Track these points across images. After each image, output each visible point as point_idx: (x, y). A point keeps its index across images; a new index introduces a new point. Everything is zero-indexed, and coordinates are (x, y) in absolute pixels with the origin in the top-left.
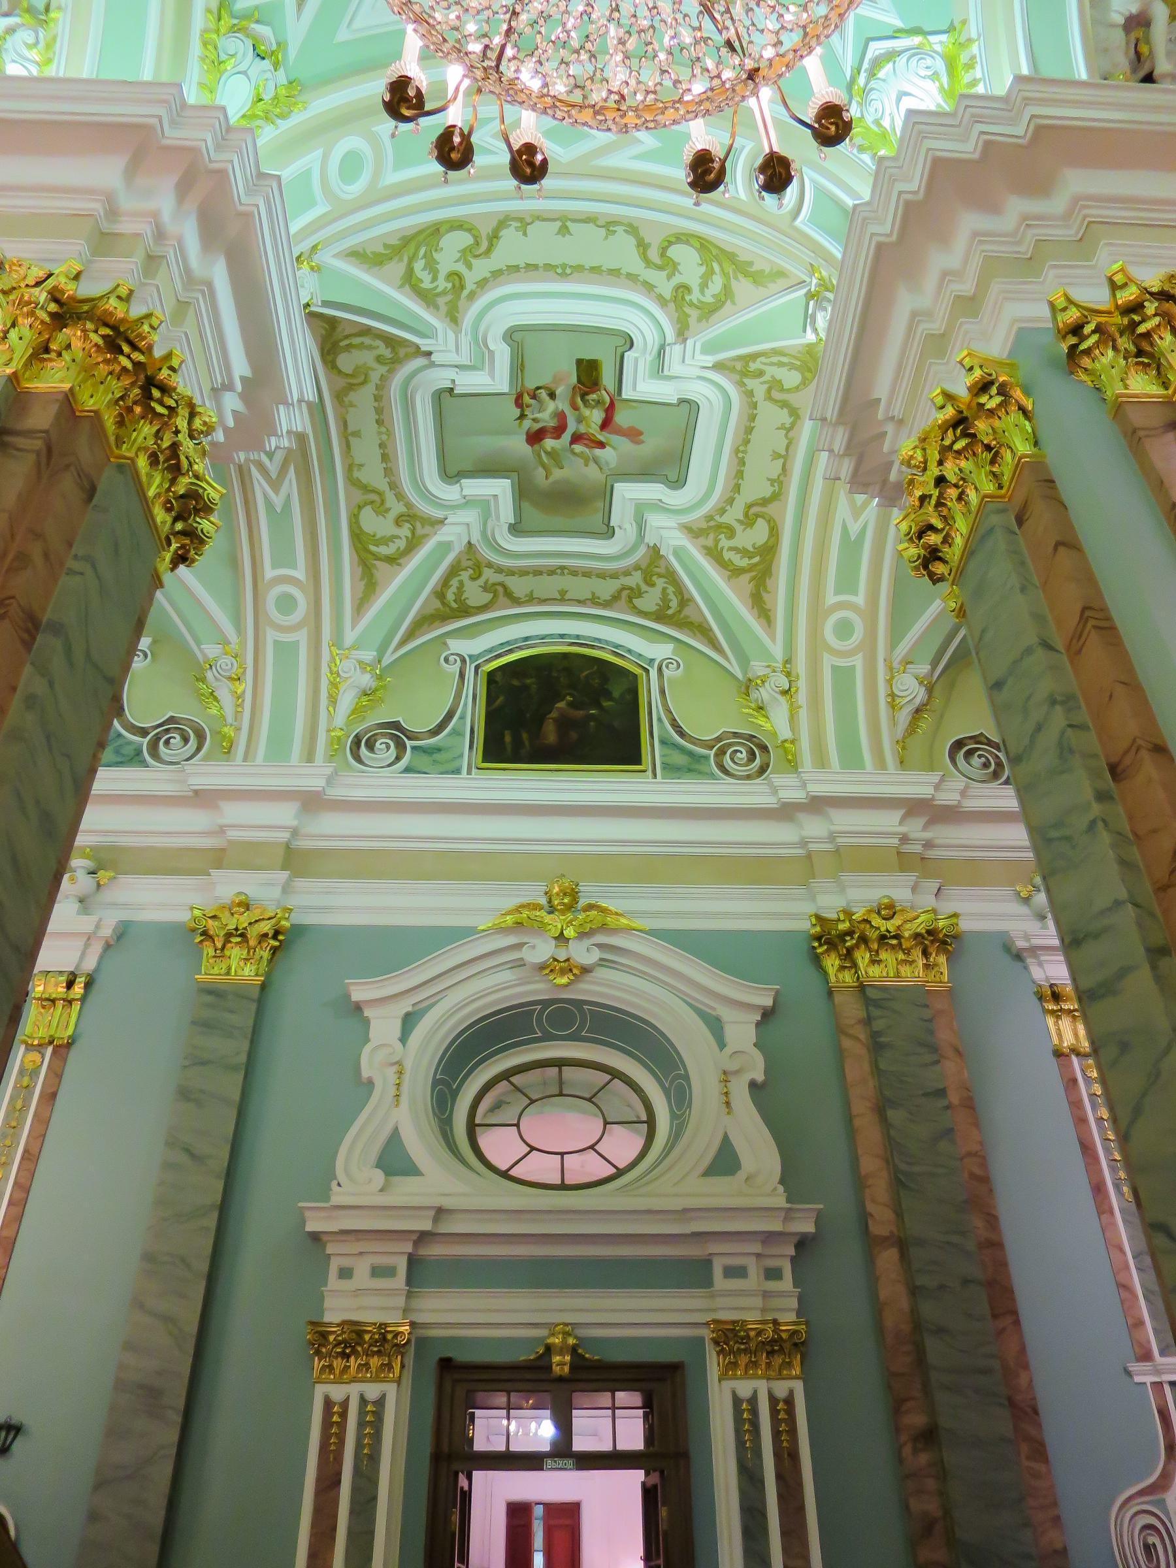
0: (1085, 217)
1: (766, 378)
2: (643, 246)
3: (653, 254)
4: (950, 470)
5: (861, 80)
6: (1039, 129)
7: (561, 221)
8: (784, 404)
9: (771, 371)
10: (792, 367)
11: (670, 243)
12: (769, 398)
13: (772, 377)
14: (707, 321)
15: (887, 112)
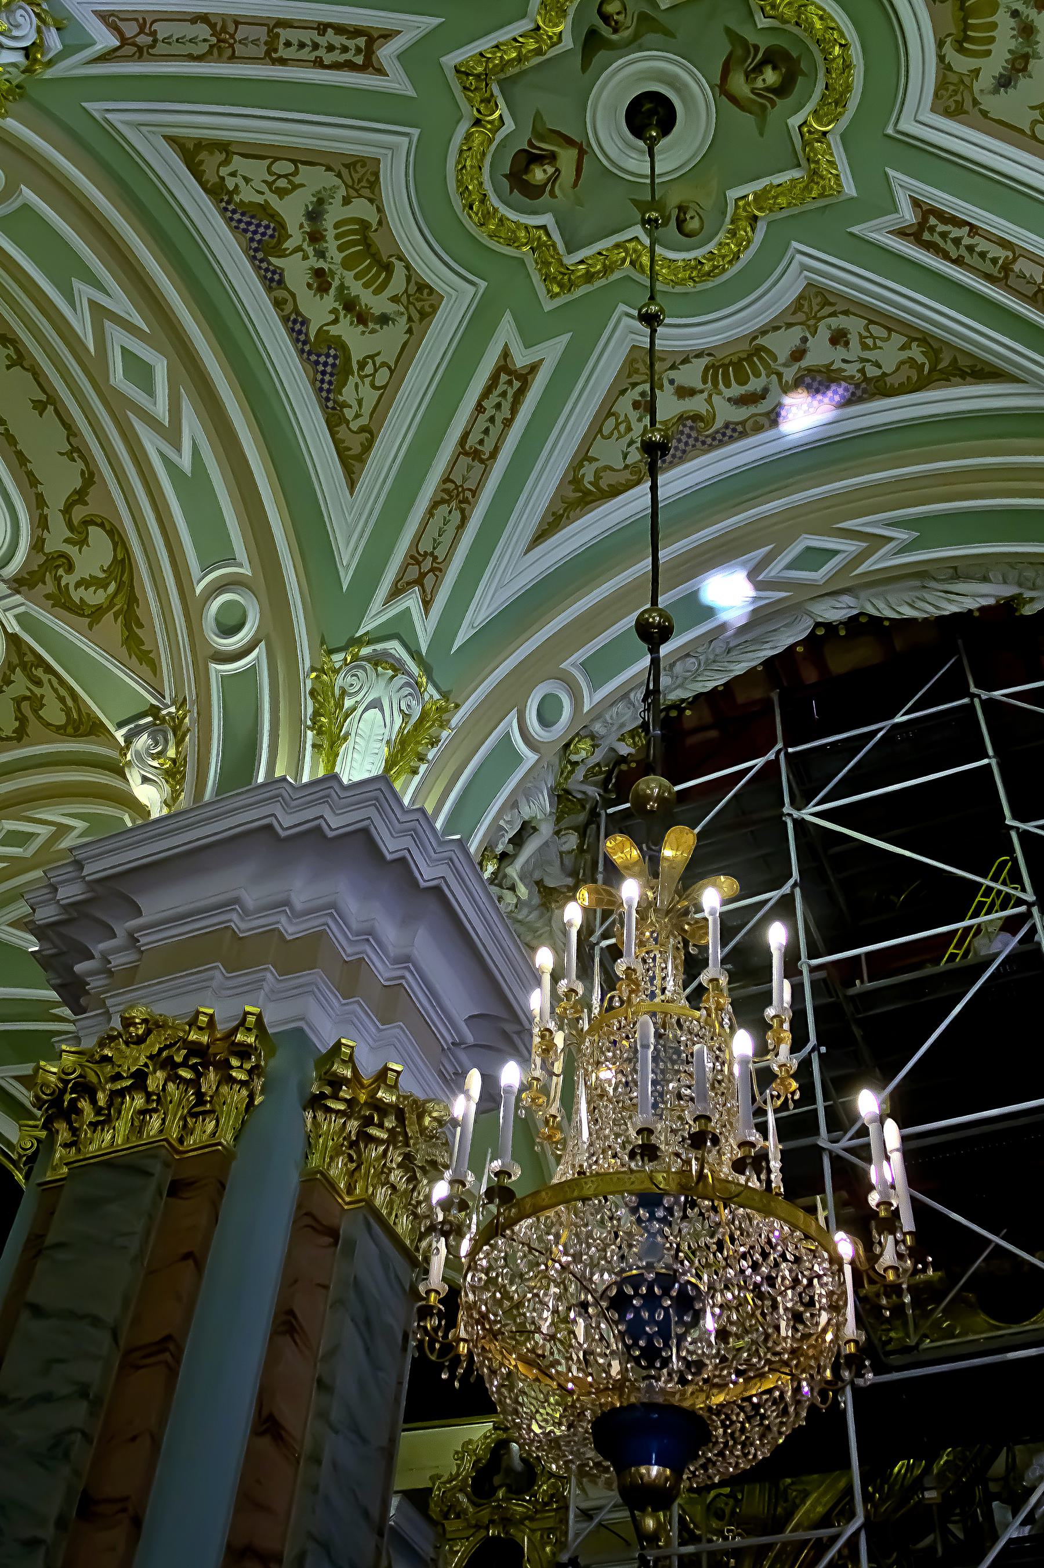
0: (403, 977)
1: (38, 691)
2: (79, 497)
3: (79, 513)
4: (156, 1080)
5: (365, 651)
6: (437, 889)
7: (48, 399)
8: (22, 720)
9: (46, 691)
10: (68, 711)
11: (102, 525)
12: (18, 701)
13: (42, 696)
14: (53, 606)
15: (358, 698)
